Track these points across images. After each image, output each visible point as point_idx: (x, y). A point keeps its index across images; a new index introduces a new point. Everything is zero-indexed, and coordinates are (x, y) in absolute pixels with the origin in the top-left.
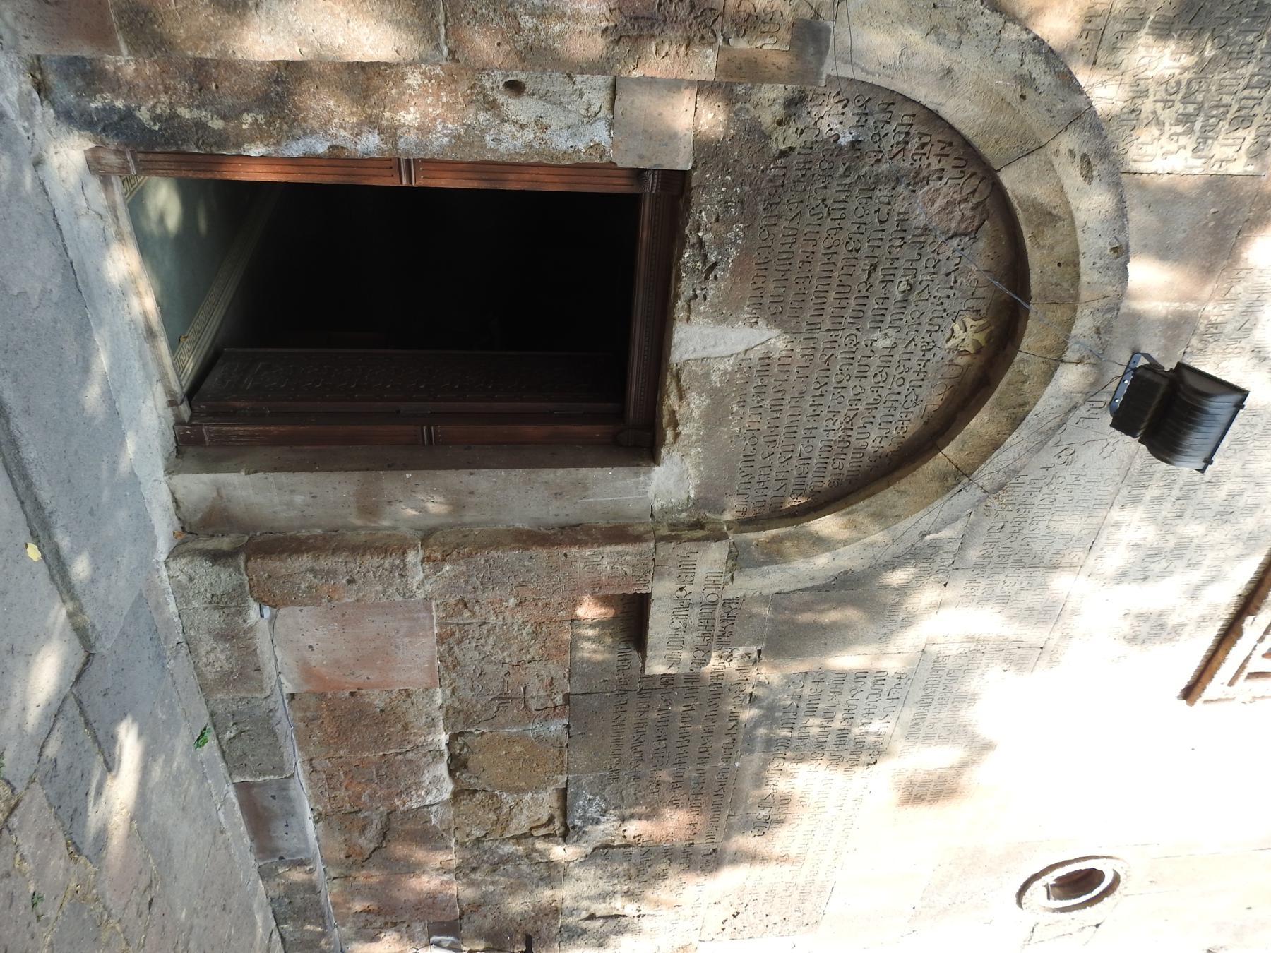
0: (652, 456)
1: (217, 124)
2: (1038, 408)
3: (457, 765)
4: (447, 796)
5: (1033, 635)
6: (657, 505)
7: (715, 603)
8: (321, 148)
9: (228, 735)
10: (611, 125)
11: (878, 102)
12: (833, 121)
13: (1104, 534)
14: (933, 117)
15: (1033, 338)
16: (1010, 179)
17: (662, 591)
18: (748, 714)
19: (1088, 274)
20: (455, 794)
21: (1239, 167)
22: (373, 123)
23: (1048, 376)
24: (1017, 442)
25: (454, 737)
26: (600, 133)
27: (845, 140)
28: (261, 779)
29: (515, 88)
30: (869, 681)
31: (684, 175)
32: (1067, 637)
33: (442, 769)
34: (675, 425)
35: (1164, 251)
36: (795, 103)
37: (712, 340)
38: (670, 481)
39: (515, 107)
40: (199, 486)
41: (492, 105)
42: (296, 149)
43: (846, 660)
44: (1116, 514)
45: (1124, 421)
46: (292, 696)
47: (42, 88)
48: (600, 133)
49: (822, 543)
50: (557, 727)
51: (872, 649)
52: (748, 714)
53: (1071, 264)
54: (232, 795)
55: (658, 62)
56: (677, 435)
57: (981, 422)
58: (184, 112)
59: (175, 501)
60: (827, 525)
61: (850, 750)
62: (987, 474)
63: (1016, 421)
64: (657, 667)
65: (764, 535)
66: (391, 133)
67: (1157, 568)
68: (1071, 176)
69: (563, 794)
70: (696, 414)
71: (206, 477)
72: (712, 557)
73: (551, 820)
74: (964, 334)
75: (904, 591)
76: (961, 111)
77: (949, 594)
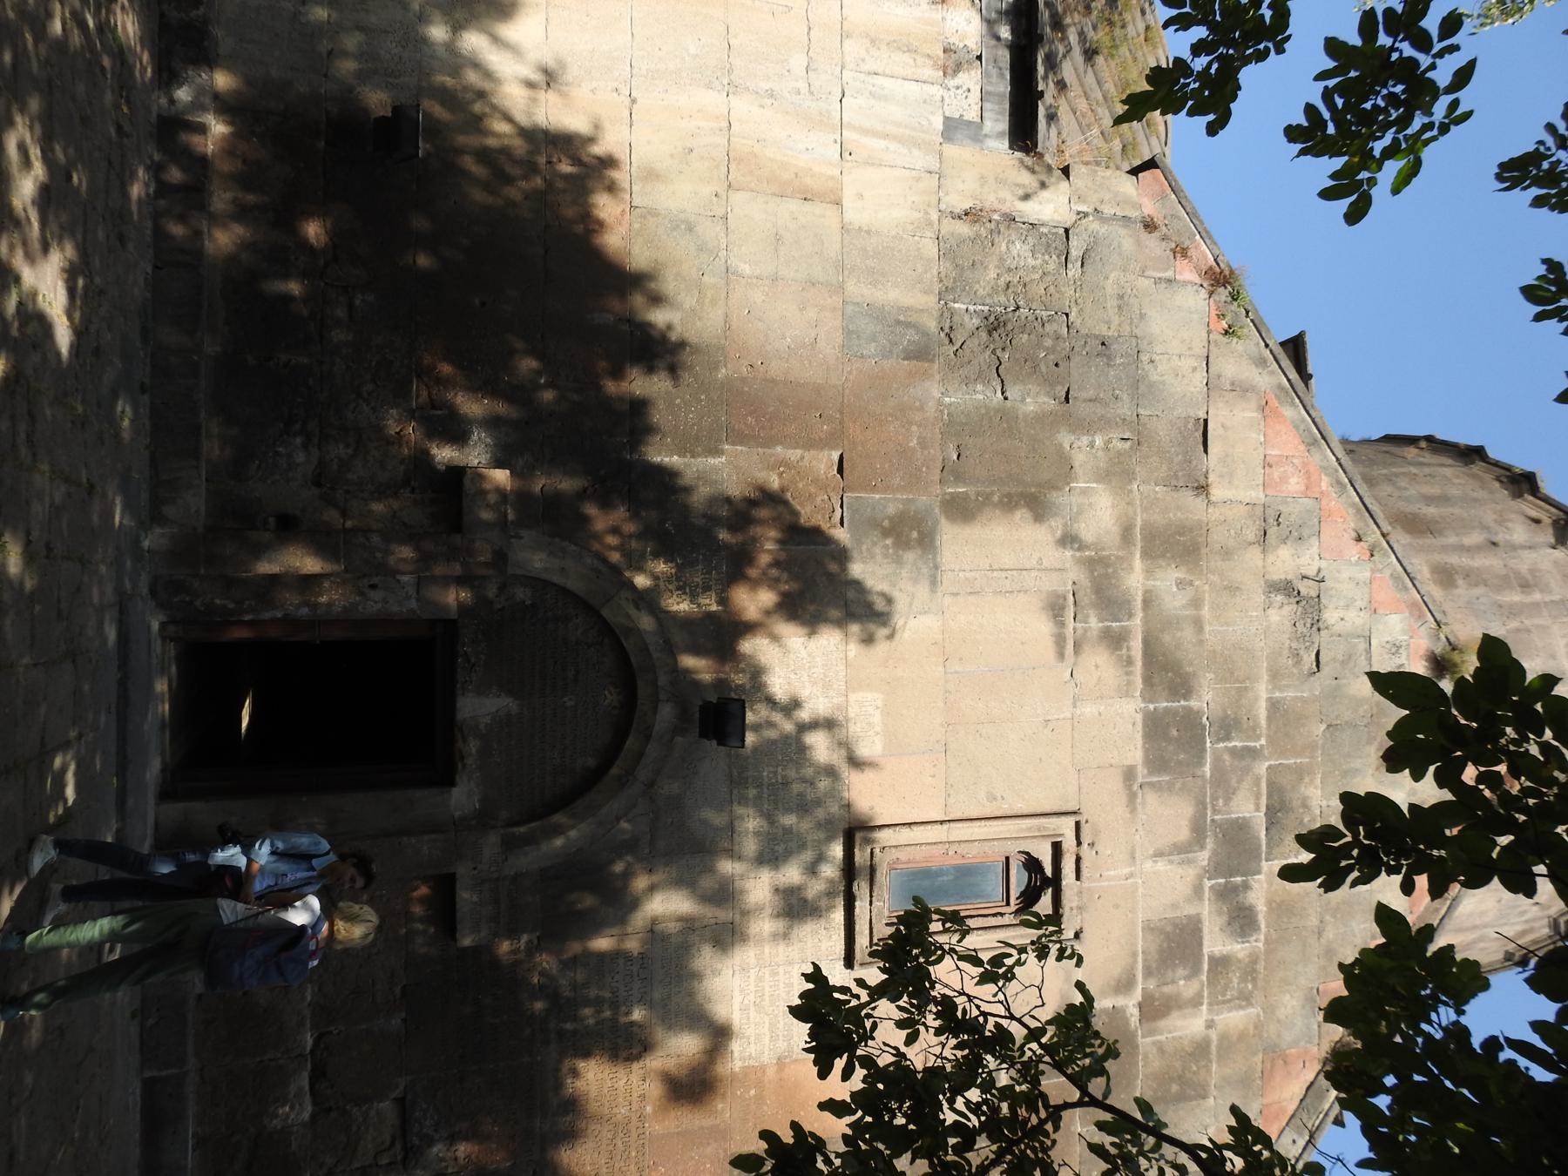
0: (452, 783)
1: (231, 606)
2: (657, 728)
3: (317, 1075)
4: (306, 1116)
5: (723, 915)
6: (457, 814)
7: (497, 879)
8: (279, 615)
9: (150, 1022)
10: (418, 600)
11: (538, 583)
12: (522, 594)
13: (736, 823)
14: (564, 591)
15: (643, 691)
16: (605, 613)
17: (463, 870)
18: (539, 1005)
19: (656, 655)
20: (313, 1116)
21: (714, 608)
22: (306, 603)
23: (655, 709)
24: (653, 751)
25: (317, 1041)
26: (413, 604)
27: (528, 602)
28: (164, 1073)
29: (373, 587)
30: (621, 961)
31: (454, 622)
32: (745, 913)
33: (304, 1080)
34: (462, 758)
35: (697, 651)
36: (502, 588)
37: (478, 707)
38: (463, 797)
39: (373, 594)
40: (174, 810)
41: (362, 594)
42: (267, 615)
43: (602, 943)
44: (740, 810)
45: (704, 734)
46: (200, 996)
47: (153, 592)
48: (413, 604)
49: (558, 830)
50: (396, 1022)
51: (614, 931)
52: (539, 1005)
53: (645, 649)
54: (138, 1091)
55: (439, 570)
56: (464, 766)
57: (631, 743)
58: (218, 601)
59: (156, 824)
60: (559, 818)
61: (627, 1045)
62: (643, 774)
63: (648, 738)
64: (467, 942)
65: (523, 829)
66: (316, 606)
67: (780, 848)
68: (632, 611)
69: (401, 1102)
70: (474, 751)
71: (180, 806)
72: (491, 843)
73: (392, 1144)
74: (610, 697)
75: (627, 875)
76: (573, 584)
77: (655, 878)
